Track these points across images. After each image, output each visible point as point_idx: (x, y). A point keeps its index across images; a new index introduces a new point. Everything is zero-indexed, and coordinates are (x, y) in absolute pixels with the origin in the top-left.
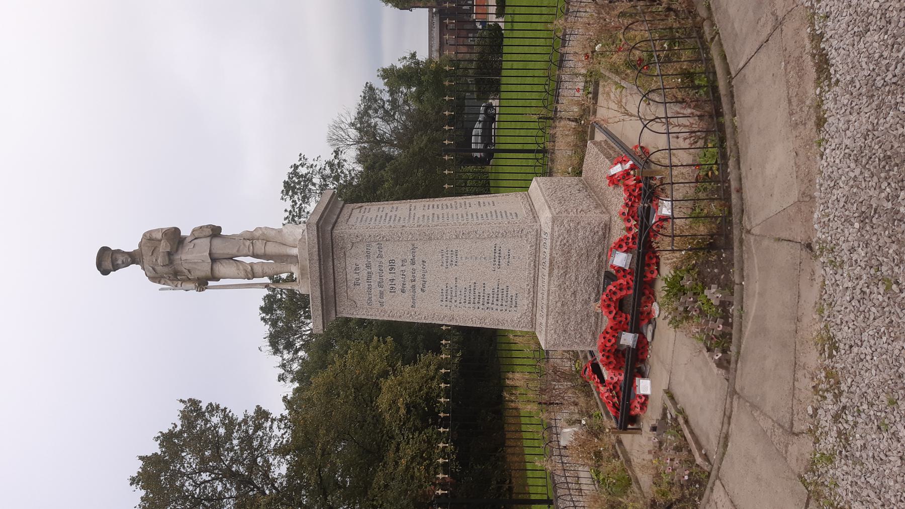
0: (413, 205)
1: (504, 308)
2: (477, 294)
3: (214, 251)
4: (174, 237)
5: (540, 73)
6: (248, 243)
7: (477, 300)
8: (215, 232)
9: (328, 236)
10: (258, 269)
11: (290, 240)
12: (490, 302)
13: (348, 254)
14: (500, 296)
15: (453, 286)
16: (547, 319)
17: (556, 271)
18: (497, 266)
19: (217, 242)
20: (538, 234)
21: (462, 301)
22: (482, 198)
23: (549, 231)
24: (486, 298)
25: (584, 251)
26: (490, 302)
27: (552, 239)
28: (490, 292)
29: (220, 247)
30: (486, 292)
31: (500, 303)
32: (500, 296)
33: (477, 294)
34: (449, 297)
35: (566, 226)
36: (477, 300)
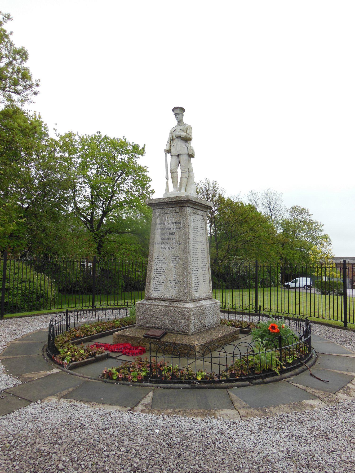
0: (205, 244)
1: (154, 285)
2: (160, 273)
3: (182, 155)
4: (187, 140)
5: (272, 307)
6: (187, 170)
7: (158, 272)
8: (191, 156)
9: (185, 205)
10: (175, 175)
11: (189, 188)
12: (157, 279)
13: (178, 214)
14: (159, 283)
15: (164, 261)
16: (148, 305)
17: (167, 309)
18: (171, 282)
19: (186, 157)
20: (183, 301)
21: (158, 266)
22: (208, 277)
23: (185, 306)
24: (158, 277)
25: (175, 322)
26: (157, 279)
27: (181, 307)
28: (161, 279)
29: (184, 158)
30: (161, 277)
31: (156, 283)
32: (159, 283)
33: (160, 273)
34: (159, 260)
35: (187, 314)
36: (158, 272)
